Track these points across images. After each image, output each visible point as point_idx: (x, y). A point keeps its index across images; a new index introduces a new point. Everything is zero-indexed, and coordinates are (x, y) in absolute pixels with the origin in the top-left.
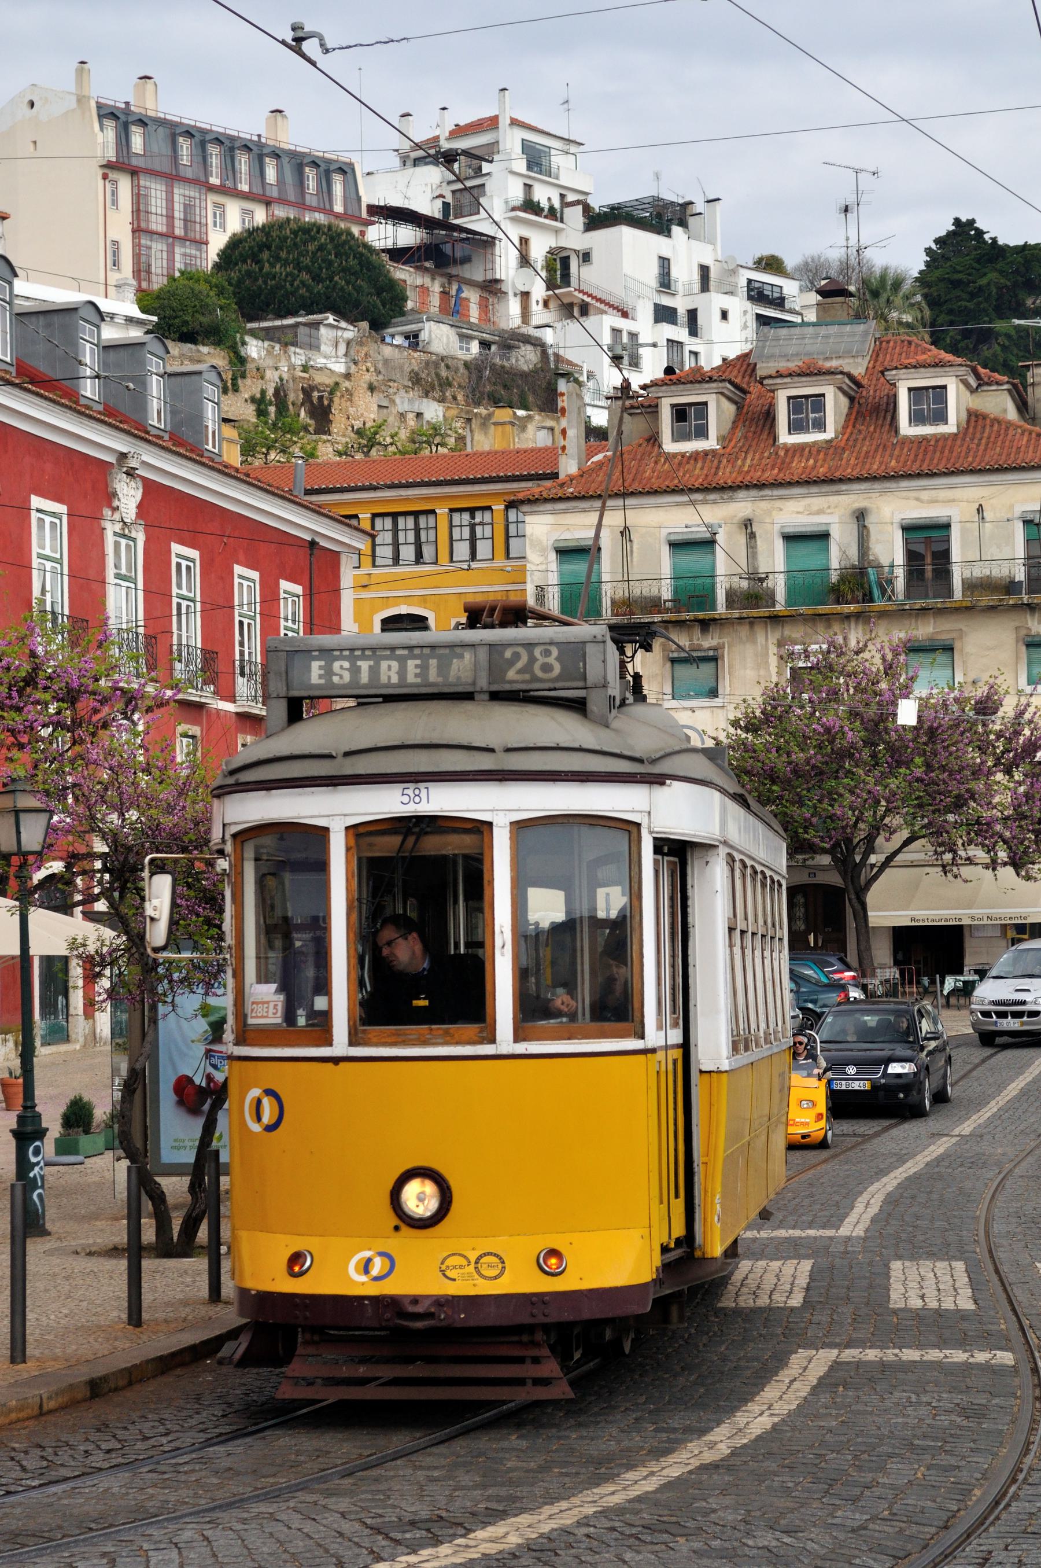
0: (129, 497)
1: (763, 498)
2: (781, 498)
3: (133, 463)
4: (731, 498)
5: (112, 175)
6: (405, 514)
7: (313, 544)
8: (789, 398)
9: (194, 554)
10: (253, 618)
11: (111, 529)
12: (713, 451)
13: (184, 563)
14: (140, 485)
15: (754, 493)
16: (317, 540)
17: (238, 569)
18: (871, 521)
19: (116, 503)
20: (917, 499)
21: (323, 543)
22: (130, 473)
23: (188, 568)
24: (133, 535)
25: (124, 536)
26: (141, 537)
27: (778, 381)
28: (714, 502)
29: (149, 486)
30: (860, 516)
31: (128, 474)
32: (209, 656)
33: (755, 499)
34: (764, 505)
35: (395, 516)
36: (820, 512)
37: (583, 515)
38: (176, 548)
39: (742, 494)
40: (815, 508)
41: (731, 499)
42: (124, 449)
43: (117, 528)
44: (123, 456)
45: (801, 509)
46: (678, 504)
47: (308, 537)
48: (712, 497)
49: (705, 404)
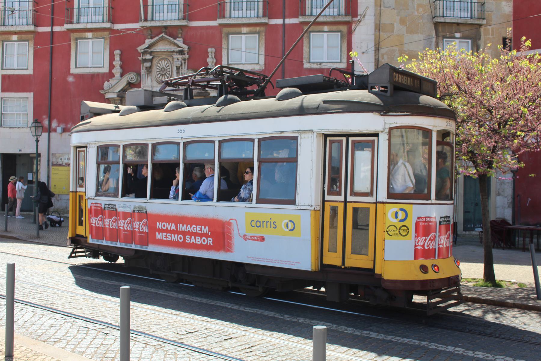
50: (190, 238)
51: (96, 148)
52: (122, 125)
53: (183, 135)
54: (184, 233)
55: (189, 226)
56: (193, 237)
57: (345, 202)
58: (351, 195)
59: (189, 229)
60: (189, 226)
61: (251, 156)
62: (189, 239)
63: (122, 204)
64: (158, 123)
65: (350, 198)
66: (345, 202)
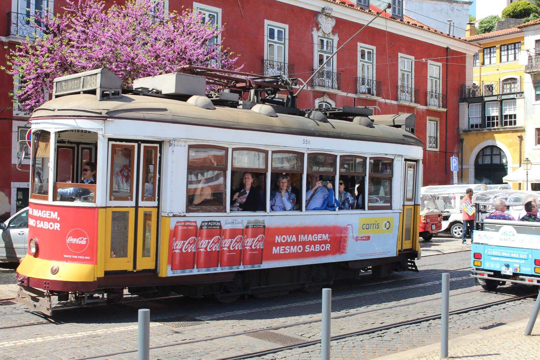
0: (327, 25)
3: (327, 11)
7: (447, 48)
9: (374, 48)
11: (316, 35)
13: (366, 51)
14: (334, 20)
17: (400, 54)
19: (319, 26)
21: (452, 48)
22: (328, 16)
23: (369, 53)
25: (325, 37)
26: (336, 39)
31: (325, 15)
32: (379, 83)
43: (320, 34)
44: (323, 9)
47: (446, 47)
50: (310, 248)
51: (187, 147)
52: (232, 124)
53: (308, 146)
54: (304, 244)
55: (310, 236)
56: (313, 246)
57: (137, 207)
58: (143, 200)
59: (310, 238)
60: (310, 236)
61: (262, 167)
62: (308, 249)
63: (230, 220)
64: (281, 130)
65: (141, 203)
66: (137, 207)
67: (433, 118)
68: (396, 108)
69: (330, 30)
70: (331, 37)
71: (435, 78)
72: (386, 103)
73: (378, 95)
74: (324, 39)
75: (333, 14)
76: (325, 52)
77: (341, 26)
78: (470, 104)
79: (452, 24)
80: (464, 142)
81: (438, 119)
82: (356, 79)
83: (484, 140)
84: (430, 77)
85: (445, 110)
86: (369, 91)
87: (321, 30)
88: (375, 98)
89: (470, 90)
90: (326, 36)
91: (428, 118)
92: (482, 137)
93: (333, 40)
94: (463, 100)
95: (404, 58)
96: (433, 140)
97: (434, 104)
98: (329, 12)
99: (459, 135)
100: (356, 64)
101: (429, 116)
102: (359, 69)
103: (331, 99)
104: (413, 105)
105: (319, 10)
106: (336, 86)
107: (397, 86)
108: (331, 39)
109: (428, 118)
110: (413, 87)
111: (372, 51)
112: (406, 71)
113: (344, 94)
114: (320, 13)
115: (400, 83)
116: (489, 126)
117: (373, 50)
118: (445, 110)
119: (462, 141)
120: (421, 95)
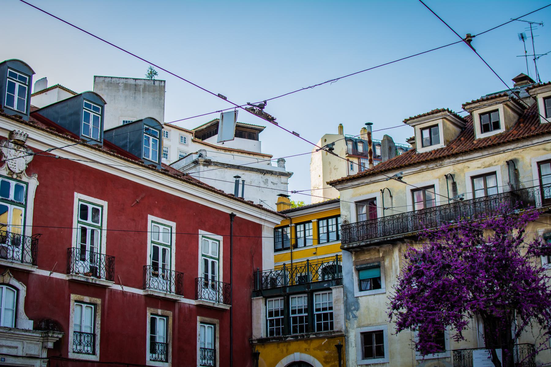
1: (458, 162)
2: (468, 160)
3: (18, 137)
4: (441, 165)
5: (351, 159)
6: (331, 217)
7: (232, 215)
8: (481, 115)
9: (105, 204)
10: (170, 246)
12: (442, 149)
13: (90, 207)
15: (453, 160)
16: (235, 213)
17: (150, 218)
18: (519, 167)
20: (545, 149)
21: (238, 215)
22: (20, 144)
24: (25, 179)
25: (12, 179)
26: (33, 183)
27: (473, 106)
28: (433, 169)
29: (37, 153)
30: (512, 164)
31: (15, 143)
32: (110, 260)
33: (455, 163)
34: (460, 166)
35: (327, 219)
36: (489, 166)
37: (367, 186)
38: (77, 196)
39: (447, 161)
40: (487, 164)
41: (442, 166)
42: (12, 129)
44: (11, 133)
45: (480, 166)
46: (414, 173)
47: (229, 212)
48: (431, 166)
49: (437, 125)
67: (207, 319)
68: (143, 300)
69: (23, 167)
70: (25, 179)
71: (211, 258)
72: (123, 293)
73: (109, 278)
74: (10, 181)
75: (29, 143)
76: (12, 202)
77: (41, 162)
78: (268, 300)
79: (241, 182)
80: (260, 358)
81: (216, 321)
82: (69, 252)
83: (288, 353)
84: (203, 255)
85: (227, 307)
86: (94, 271)
87: (5, 166)
88: (103, 281)
89: (267, 277)
90: (15, 176)
91: (199, 318)
92: (285, 350)
93: (27, 184)
94: (257, 293)
95: (158, 223)
96: (208, 354)
97: (209, 296)
98: (22, 138)
99: (252, 345)
100: (71, 228)
101: (201, 315)
102: (76, 235)
103: (19, 280)
104: (173, 296)
105: (6, 135)
106: (28, 258)
107: (145, 266)
108: (25, 183)
109: (199, 318)
110: (173, 268)
111: (100, 208)
112: (161, 244)
113: (46, 273)
114: (5, 139)
115: (149, 262)
116: (295, 331)
117: (102, 207)
118: (227, 307)
119: (256, 355)
120: (186, 283)
